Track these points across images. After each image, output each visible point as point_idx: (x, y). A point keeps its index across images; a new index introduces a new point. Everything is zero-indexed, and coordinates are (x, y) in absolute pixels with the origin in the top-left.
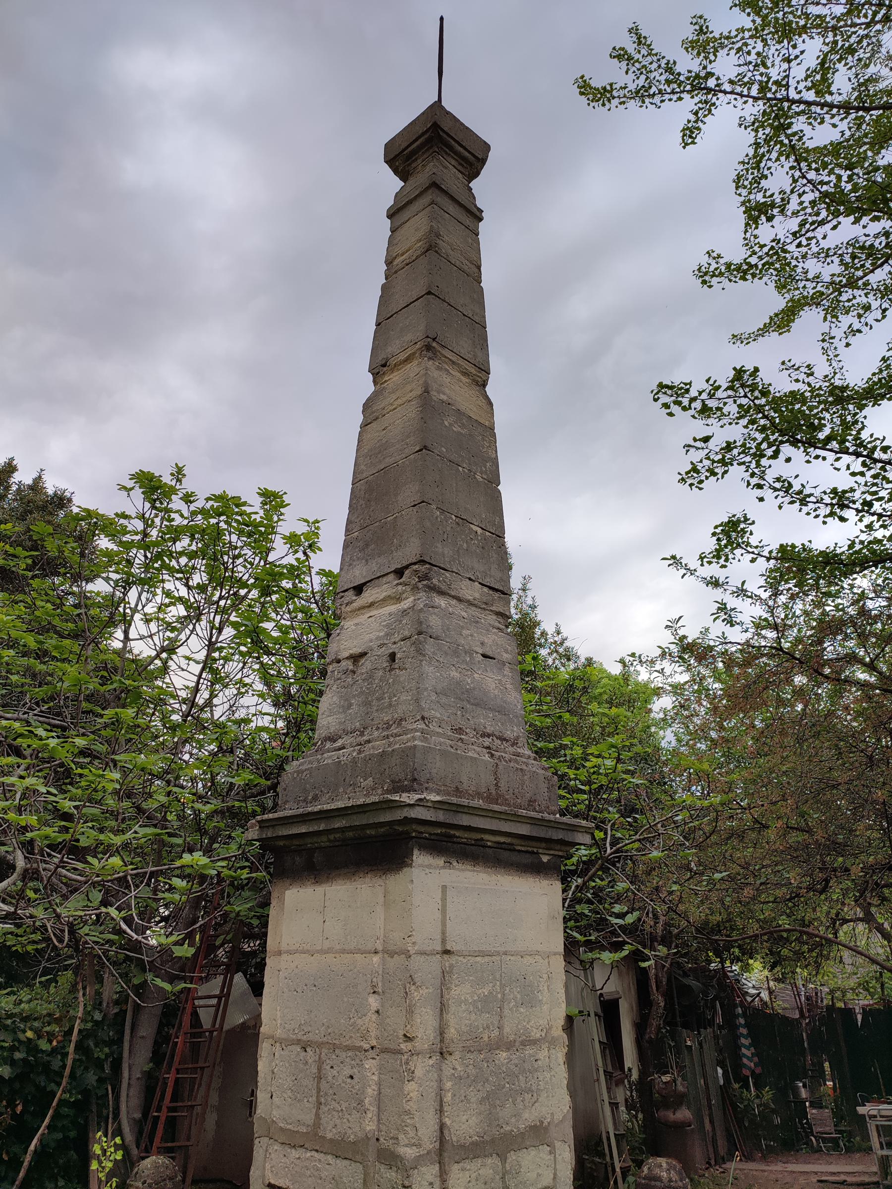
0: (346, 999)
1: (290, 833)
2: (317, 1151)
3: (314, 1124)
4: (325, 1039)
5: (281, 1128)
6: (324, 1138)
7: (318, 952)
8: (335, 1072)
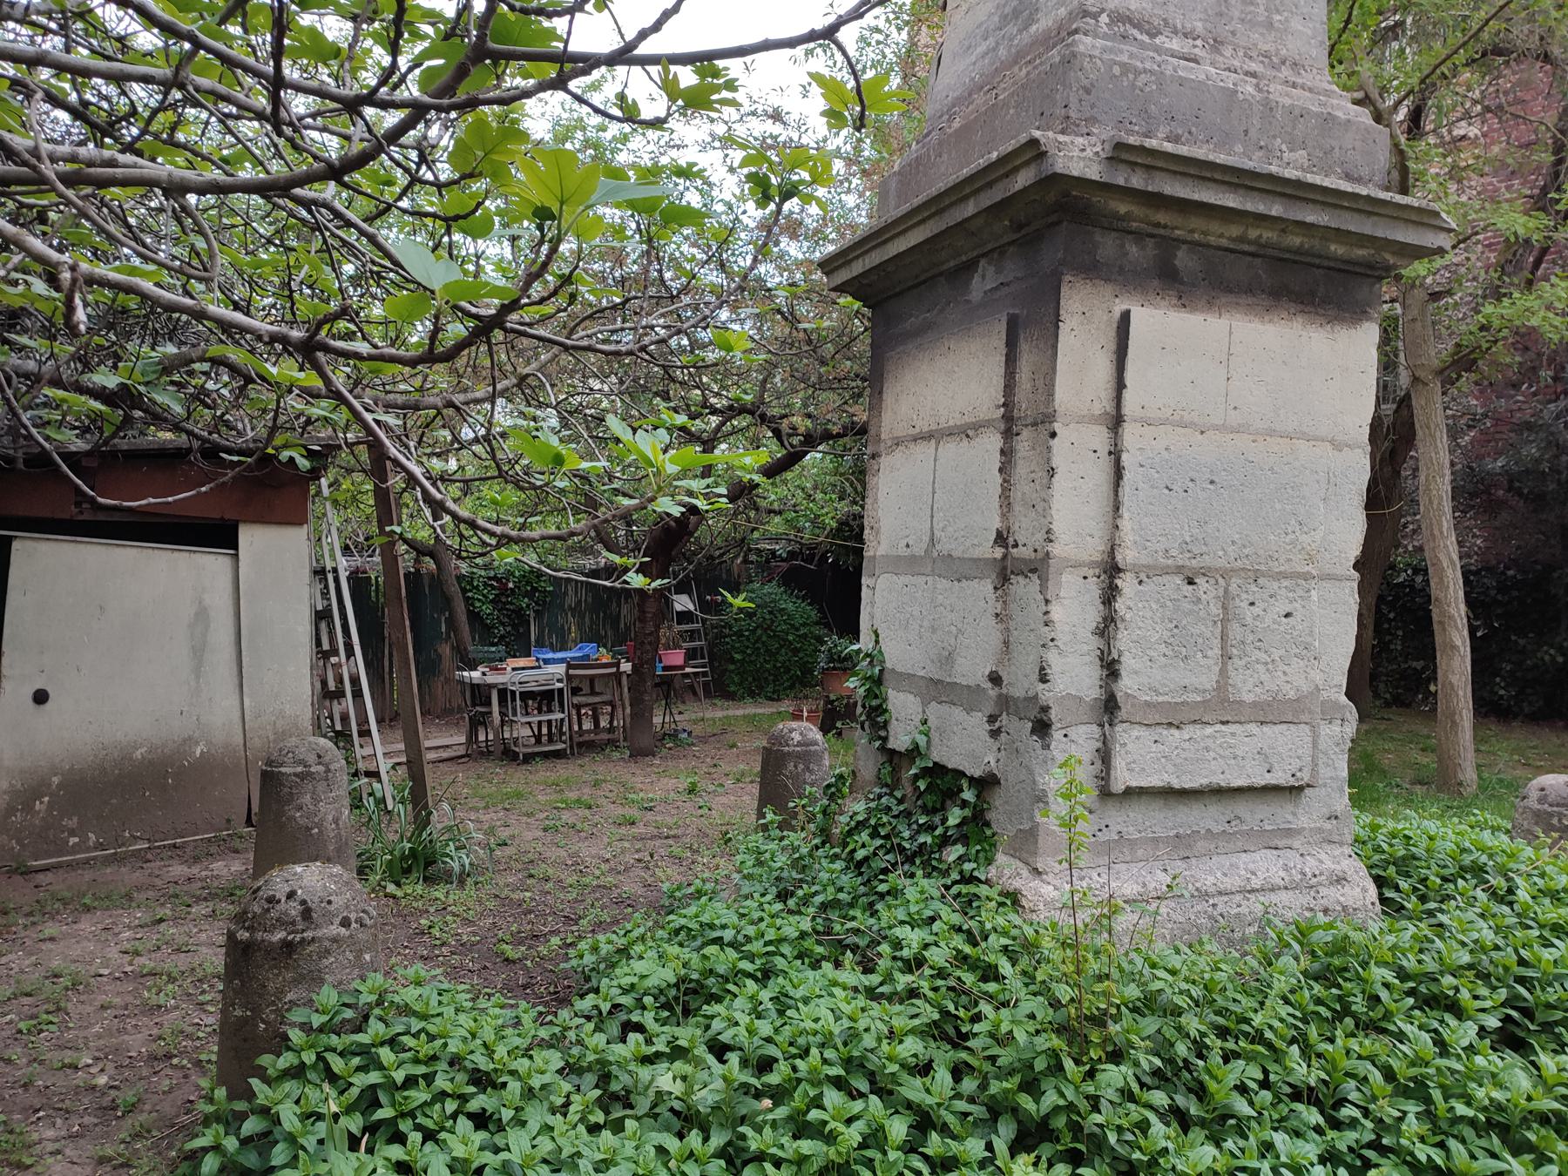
0: (1278, 506)
1: (1196, 197)
2: (1223, 723)
3: (1218, 689)
4: (1239, 564)
5: (1148, 704)
6: (1241, 703)
7: (1216, 428)
8: (1256, 610)
